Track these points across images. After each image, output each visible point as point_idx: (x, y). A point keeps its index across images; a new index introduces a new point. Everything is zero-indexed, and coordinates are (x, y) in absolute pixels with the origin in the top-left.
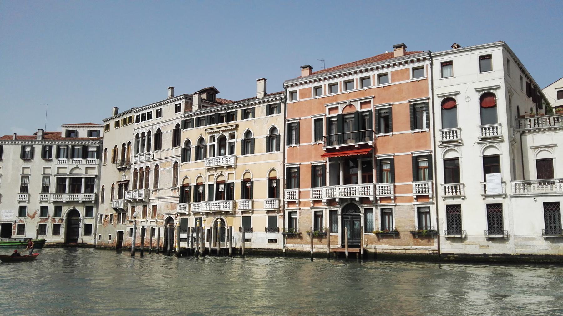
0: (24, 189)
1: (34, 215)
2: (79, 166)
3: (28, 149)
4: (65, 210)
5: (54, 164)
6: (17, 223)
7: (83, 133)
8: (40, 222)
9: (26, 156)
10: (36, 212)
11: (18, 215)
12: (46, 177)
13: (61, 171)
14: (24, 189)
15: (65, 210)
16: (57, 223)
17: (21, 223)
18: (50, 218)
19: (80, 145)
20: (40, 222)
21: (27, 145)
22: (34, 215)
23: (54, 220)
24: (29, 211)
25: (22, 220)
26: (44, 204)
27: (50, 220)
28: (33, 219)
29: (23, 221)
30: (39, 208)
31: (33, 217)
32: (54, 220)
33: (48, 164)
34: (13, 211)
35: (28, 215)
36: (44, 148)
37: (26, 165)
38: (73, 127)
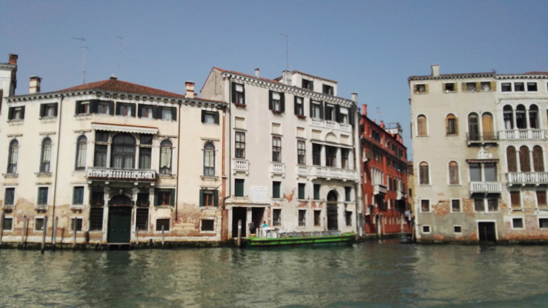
0: (276, 156)
1: (292, 195)
2: (334, 132)
3: (276, 97)
4: (324, 191)
5: (309, 123)
6: (272, 208)
7: (318, 87)
8: (299, 206)
9: (277, 106)
10: (293, 192)
11: (271, 195)
12: (301, 141)
13: (316, 136)
14: (276, 156)
15: (324, 191)
16: (317, 209)
17: (277, 208)
18: (310, 201)
19: (333, 103)
20: (299, 206)
21: (275, 90)
22: (292, 195)
23: (314, 204)
24: (283, 190)
25: (278, 202)
26: (302, 181)
27: (309, 204)
28: (291, 202)
29: (278, 205)
30: (297, 186)
31: (290, 199)
32: (314, 204)
33: (301, 124)
34: (266, 188)
35: (285, 196)
36: (296, 98)
37: (277, 120)
38: (308, 75)
